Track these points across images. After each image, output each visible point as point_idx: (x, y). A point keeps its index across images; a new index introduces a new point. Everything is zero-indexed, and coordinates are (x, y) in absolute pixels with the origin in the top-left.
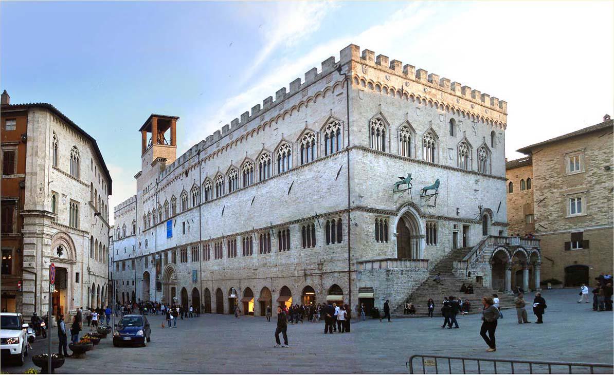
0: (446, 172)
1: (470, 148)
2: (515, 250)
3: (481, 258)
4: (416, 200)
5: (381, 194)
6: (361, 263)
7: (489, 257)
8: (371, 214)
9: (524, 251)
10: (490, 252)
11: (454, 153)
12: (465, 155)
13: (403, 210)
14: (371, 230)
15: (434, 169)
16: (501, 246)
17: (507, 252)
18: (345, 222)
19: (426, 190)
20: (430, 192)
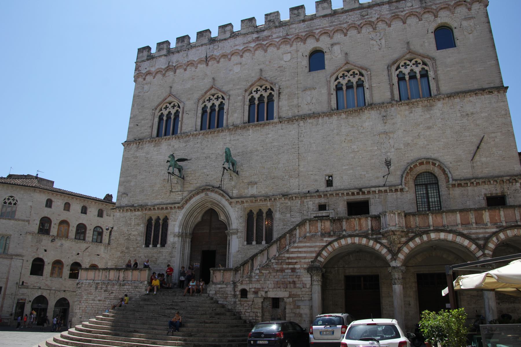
1: (364, 72)
2: (406, 243)
3: (277, 264)
7: (310, 260)
9: (459, 239)
10: (309, 249)
14: (136, 233)
16: (350, 236)
17: (378, 246)
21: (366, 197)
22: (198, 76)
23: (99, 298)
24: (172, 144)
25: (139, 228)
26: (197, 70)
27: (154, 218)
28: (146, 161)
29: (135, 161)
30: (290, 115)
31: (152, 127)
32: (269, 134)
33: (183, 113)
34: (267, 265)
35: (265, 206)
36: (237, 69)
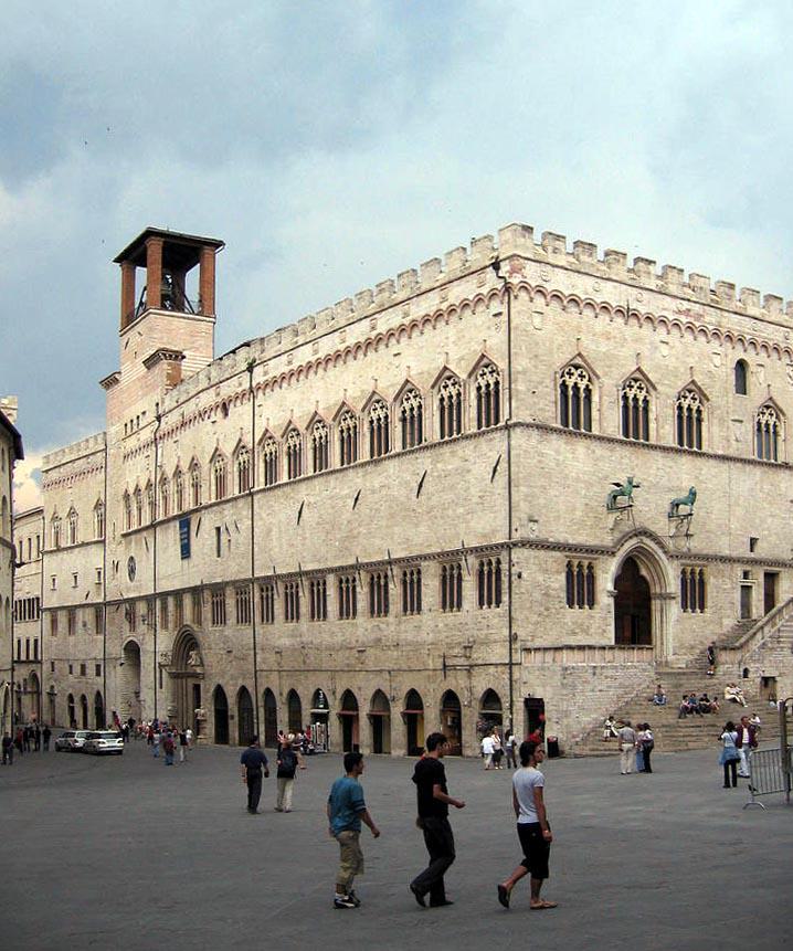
0: (725, 466)
1: (782, 417)
4: (663, 527)
5: (578, 513)
6: (528, 650)
8: (557, 554)
11: (747, 431)
12: (772, 430)
13: (633, 542)
14: (557, 586)
15: (699, 461)
18: (504, 566)
19: (677, 505)
20: (683, 509)
21: (777, 569)
22: (615, 337)
23: (600, 688)
24: (592, 447)
25: (559, 577)
26: (614, 325)
27: (576, 563)
28: (557, 465)
29: (540, 462)
30: (720, 452)
31: (556, 403)
32: (701, 469)
33: (600, 398)
34: (764, 644)
35: (697, 564)
36: (664, 350)
